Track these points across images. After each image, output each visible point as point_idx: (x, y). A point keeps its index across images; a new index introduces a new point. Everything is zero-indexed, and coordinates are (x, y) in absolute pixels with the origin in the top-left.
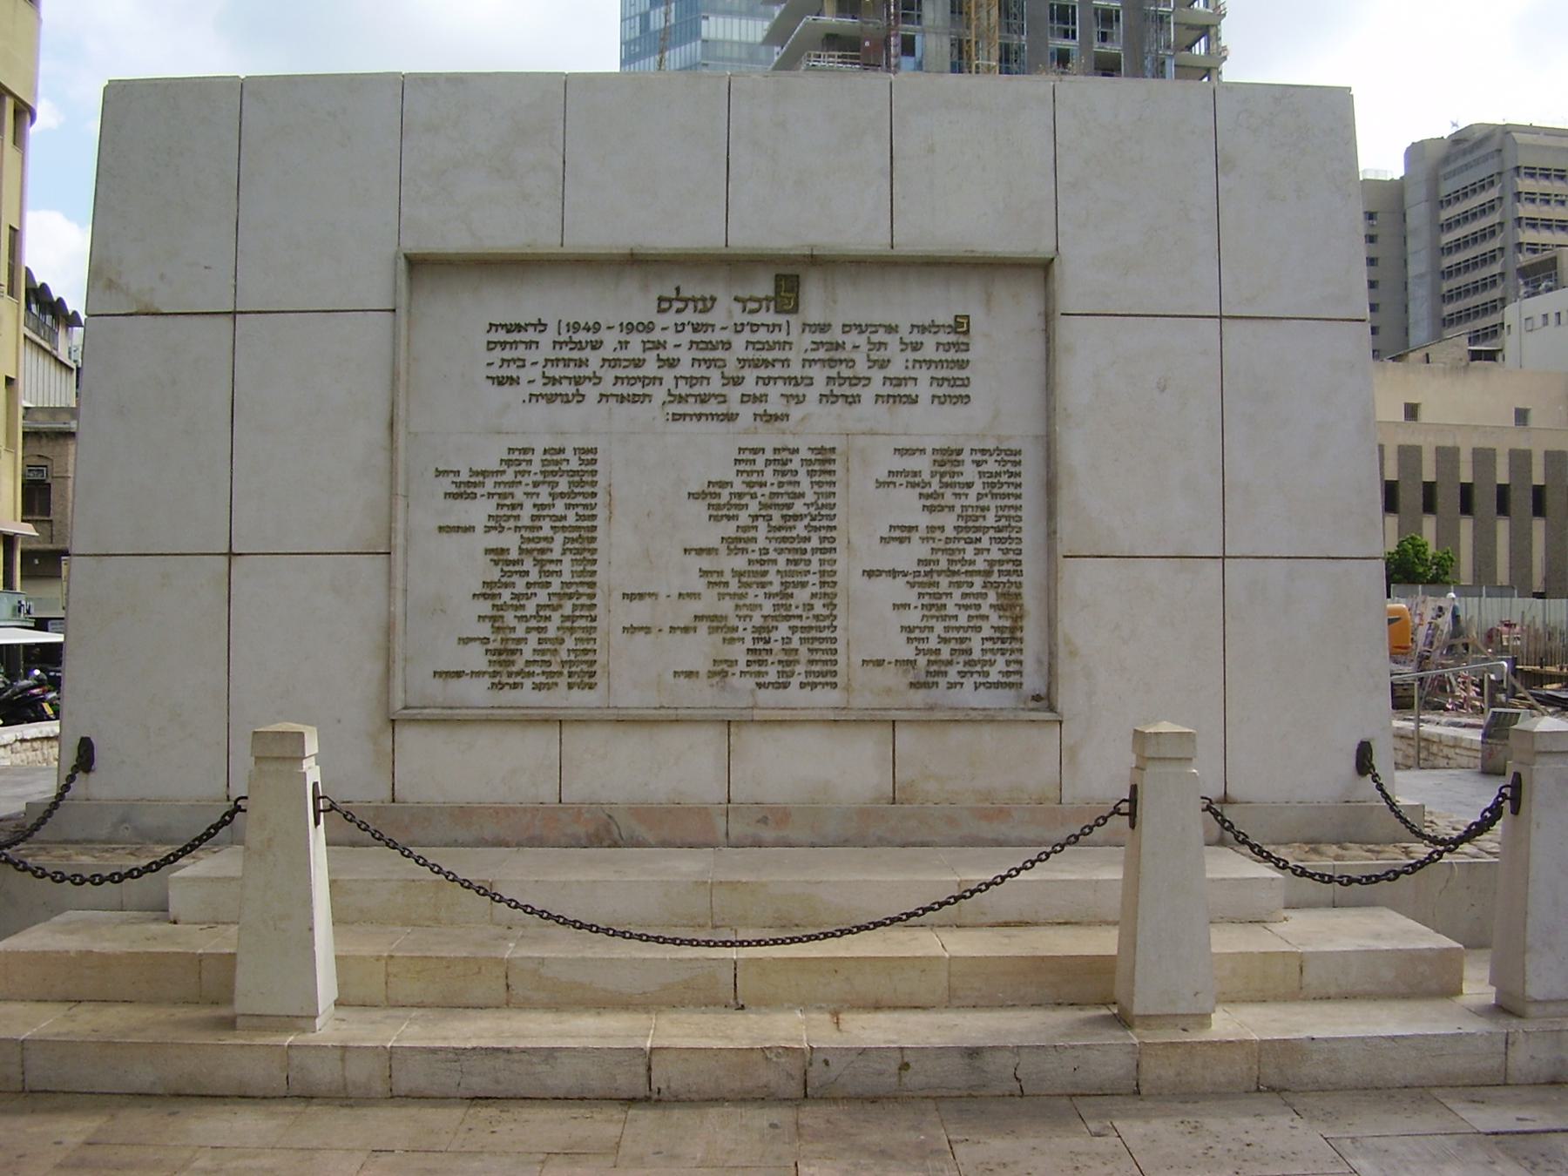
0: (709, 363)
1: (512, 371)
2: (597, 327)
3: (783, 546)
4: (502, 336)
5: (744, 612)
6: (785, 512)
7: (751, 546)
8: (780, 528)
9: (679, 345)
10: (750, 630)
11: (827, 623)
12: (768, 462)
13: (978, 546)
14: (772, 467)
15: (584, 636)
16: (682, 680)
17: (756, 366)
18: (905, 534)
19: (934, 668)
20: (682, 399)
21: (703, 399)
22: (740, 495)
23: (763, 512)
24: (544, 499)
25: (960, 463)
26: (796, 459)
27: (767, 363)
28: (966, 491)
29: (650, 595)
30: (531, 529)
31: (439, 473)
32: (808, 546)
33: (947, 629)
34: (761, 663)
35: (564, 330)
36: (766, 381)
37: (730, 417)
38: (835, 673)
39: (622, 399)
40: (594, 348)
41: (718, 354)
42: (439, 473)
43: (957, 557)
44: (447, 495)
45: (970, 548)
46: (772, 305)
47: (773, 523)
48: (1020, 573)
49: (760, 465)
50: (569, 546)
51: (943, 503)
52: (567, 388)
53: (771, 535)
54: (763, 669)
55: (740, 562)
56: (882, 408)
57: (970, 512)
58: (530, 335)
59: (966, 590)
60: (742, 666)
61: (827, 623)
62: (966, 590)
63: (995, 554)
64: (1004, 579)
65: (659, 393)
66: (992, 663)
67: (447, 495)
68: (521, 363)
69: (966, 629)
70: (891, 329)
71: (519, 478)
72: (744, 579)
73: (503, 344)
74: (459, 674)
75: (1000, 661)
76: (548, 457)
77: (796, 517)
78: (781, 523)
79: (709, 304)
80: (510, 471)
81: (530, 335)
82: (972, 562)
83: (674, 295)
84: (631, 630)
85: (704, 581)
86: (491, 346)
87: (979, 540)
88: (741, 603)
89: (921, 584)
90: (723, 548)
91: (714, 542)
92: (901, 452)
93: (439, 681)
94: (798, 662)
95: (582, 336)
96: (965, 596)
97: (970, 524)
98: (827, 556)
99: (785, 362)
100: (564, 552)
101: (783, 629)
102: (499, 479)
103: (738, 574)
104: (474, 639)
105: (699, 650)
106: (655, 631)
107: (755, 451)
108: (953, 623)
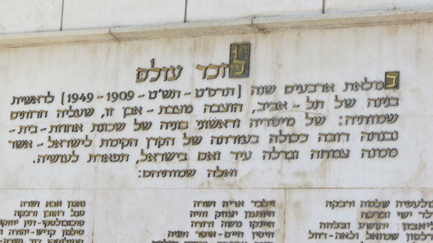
2: (90, 97)
4: (22, 107)
12: (219, 214)
14: (221, 219)
17: (212, 127)
20: (150, 158)
21: (168, 157)
25: (386, 215)
26: (241, 211)
27: (218, 124)
35: (66, 99)
36: (219, 140)
37: (189, 173)
39: (105, 158)
40: (87, 115)
46: (227, 70)
49: (211, 217)
52: (65, 150)
56: (317, 162)
58: (41, 106)
65: (134, 153)
70: (326, 88)
71: (28, 227)
73: (22, 114)
76: (50, 209)
79: (177, 72)
80: (22, 221)
81: (41, 106)
83: (148, 66)
86: (14, 115)
92: (332, 204)
95: (80, 105)
99: (237, 123)
102: (13, 227)
107: (208, 204)
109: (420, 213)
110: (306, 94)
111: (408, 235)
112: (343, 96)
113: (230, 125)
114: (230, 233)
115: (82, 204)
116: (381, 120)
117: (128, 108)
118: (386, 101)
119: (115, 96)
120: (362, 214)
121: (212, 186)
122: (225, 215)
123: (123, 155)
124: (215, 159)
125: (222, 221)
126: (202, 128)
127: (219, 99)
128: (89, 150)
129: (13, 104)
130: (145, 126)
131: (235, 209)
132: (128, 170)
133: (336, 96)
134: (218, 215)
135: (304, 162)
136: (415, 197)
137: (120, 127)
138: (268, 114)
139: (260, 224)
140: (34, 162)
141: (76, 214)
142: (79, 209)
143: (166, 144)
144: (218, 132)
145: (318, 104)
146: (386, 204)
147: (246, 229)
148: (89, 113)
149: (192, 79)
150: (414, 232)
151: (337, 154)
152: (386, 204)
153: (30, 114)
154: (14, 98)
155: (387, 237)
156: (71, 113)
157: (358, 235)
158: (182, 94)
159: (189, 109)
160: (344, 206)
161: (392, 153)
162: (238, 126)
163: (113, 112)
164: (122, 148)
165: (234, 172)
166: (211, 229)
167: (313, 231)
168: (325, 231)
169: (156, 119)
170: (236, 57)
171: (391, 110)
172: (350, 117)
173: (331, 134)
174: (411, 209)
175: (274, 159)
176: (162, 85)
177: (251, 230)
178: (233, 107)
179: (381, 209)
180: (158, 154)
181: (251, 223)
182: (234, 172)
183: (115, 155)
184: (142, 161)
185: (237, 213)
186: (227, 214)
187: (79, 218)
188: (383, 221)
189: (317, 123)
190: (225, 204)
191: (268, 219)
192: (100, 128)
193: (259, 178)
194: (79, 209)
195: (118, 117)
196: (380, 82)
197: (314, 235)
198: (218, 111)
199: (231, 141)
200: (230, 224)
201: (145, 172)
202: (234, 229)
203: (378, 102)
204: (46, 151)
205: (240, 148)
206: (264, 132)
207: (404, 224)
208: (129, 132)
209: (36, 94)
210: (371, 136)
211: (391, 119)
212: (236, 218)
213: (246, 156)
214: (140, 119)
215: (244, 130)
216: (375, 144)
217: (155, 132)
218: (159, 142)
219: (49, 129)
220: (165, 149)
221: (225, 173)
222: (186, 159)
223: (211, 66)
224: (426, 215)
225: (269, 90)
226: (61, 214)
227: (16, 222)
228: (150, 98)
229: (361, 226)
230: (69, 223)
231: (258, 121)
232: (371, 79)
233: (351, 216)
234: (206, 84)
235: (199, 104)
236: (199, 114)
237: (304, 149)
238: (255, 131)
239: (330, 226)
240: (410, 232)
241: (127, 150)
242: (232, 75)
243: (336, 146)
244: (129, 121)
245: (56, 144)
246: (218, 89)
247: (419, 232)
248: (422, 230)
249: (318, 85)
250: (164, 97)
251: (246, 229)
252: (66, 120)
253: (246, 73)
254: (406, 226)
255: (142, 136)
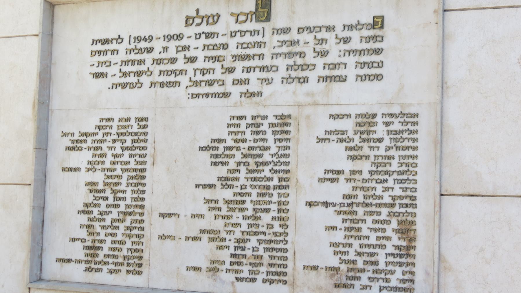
0: (216, 59)
1: (103, 69)
2: (150, 39)
3: (255, 183)
4: (99, 47)
5: (230, 228)
6: (258, 160)
7: (235, 183)
8: (254, 171)
9: (197, 48)
10: (233, 240)
11: (282, 238)
12: (249, 126)
13: (385, 185)
14: (250, 129)
15: (137, 240)
16: (192, 272)
17: (243, 60)
18: (335, 176)
19: (351, 274)
20: (196, 84)
21: (210, 83)
22: (230, 148)
23: (244, 160)
24: (119, 151)
25: (375, 124)
26: (266, 122)
27: (247, 57)
28: (378, 144)
29: (175, 214)
30: (110, 170)
31: (65, 135)
32: (271, 184)
33: (361, 246)
34: (239, 264)
36: (248, 70)
37: (226, 95)
38: (285, 274)
39: (162, 85)
40: (148, 52)
41: (220, 52)
42: (65, 135)
43: (371, 193)
44: (69, 149)
45: (379, 187)
46: (254, 16)
47: (250, 168)
48: (414, 206)
49: (243, 128)
50: (131, 181)
51: (361, 153)
52: (132, 79)
53: (249, 175)
54: (240, 268)
55: (228, 194)
56: (322, 85)
57: (380, 160)
59: (376, 217)
60: (227, 266)
61: (282, 238)
62: (376, 217)
63: (398, 192)
64: (403, 210)
65: (184, 80)
66: (392, 272)
67: (69, 149)
68: (109, 64)
69: (375, 246)
70: (329, 29)
71: (105, 137)
72: (231, 206)
73: (99, 52)
74: (69, 261)
75: (399, 270)
76: (121, 124)
77: (266, 164)
78: (255, 167)
80: (101, 133)
82: (381, 197)
83: (194, 14)
84: (162, 237)
85: (207, 206)
86: (93, 53)
87: (386, 181)
88: (228, 221)
89: (345, 213)
90: (218, 184)
91: (214, 181)
92: (334, 117)
93: (58, 264)
94: (261, 264)
95: (143, 45)
96: (375, 222)
97: (380, 169)
98: (283, 191)
99: (261, 56)
100: (127, 186)
101: (253, 241)
102: (94, 138)
103: (228, 202)
104: (78, 239)
105: (202, 253)
106: (176, 239)
107: (240, 118)
108: (366, 242)
109: (399, 122)
110: (314, 34)
111: (391, 139)
112: (341, 35)
113: (256, 58)
114: (257, 140)
115: (146, 119)
116: (371, 52)
117: (179, 46)
118: (374, 38)
119: (169, 38)
120: (357, 124)
121: (244, 104)
122: (253, 126)
123: (176, 82)
124: (245, 84)
125: (251, 131)
126: (235, 61)
127: (248, 38)
128: (151, 79)
129: (92, 45)
130: (192, 60)
131: (261, 121)
132: (180, 93)
133: (337, 35)
134: (248, 126)
135: (313, 85)
136: (396, 110)
137: (173, 61)
138: (285, 49)
139: (280, 133)
140: (109, 88)
141: (142, 127)
142: (144, 123)
143: (208, 73)
144: (248, 63)
145: (323, 41)
146: (374, 116)
147: (269, 136)
148: (150, 50)
149: (228, 23)
150: (395, 136)
151: (337, 79)
152: (374, 116)
153: (105, 52)
154: (93, 41)
155: (375, 141)
156: (136, 51)
157: (353, 139)
158: (220, 35)
159: (225, 46)
160: (343, 118)
161: (378, 77)
162: (263, 59)
163: (168, 50)
164: (175, 77)
165: (260, 94)
166: (243, 137)
167: (320, 137)
168: (329, 137)
169: (200, 54)
170: (260, 6)
171: (378, 45)
172: (347, 51)
173: (333, 64)
174: (393, 119)
175: (290, 83)
176: (205, 28)
177: (273, 137)
178: (259, 45)
179: (370, 120)
180: (203, 81)
181: (273, 132)
182: (260, 94)
183: (170, 82)
184: (190, 86)
185: (262, 124)
186: (255, 125)
187: (144, 130)
188: (372, 129)
189: (322, 56)
190: (254, 117)
191: (286, 128)
192: (158, 62)
193: (279, 98)
194: (144, 123)
195: (172, 53)
196: (369, 24)
197: (321, 140)
198: (248, 47)
199: (257, 70)
200: (258, 133)
201: (192, 95)
202: (261, 136)
203: (368, 39)
204: (118, 80)
205: (264, 75)
206: (282, 63)
207: (388, 131)
208: (180, 65)
209: (110, 37)
210: (362, 65)
211: (378, 51)
212: (262, 128)
213: (269, 82)
214: (188, 54)
215: (267, 61)
216: (366, 71)
217: (200, 64)
218: (203, 72)
219: (120, 63)
220: (207, 77)
221: (253, 95)
222: (223, 84)
223: (242, 13)
224: (404, 124)
225: (286, 31)
226: (130, 127)
227: (97, 134)
228: (196, 38)
229: (356, 132)
230: (136, 134)
231: (278, 55)
232: (363, 22)
233: (348, 125)
234: (238, 27)
235: (233, 43)
236: (233, 50)
237: (312, 75)
238: (275, 62)
239: (332, 133)
240: (392, 136)
241: (179, 78)
242: (258, 20)
243: (336, 73)
244: (180, 56)
245: (125, 74)
246: (247, 31)
247: (399, 136)
248: (401, 135)
249: (323, 26)
250: (207, 37)
251: (269, 136)
252: (133, 56)
253: (268, 18)
254: (389, 132)
255: (190, 67)
